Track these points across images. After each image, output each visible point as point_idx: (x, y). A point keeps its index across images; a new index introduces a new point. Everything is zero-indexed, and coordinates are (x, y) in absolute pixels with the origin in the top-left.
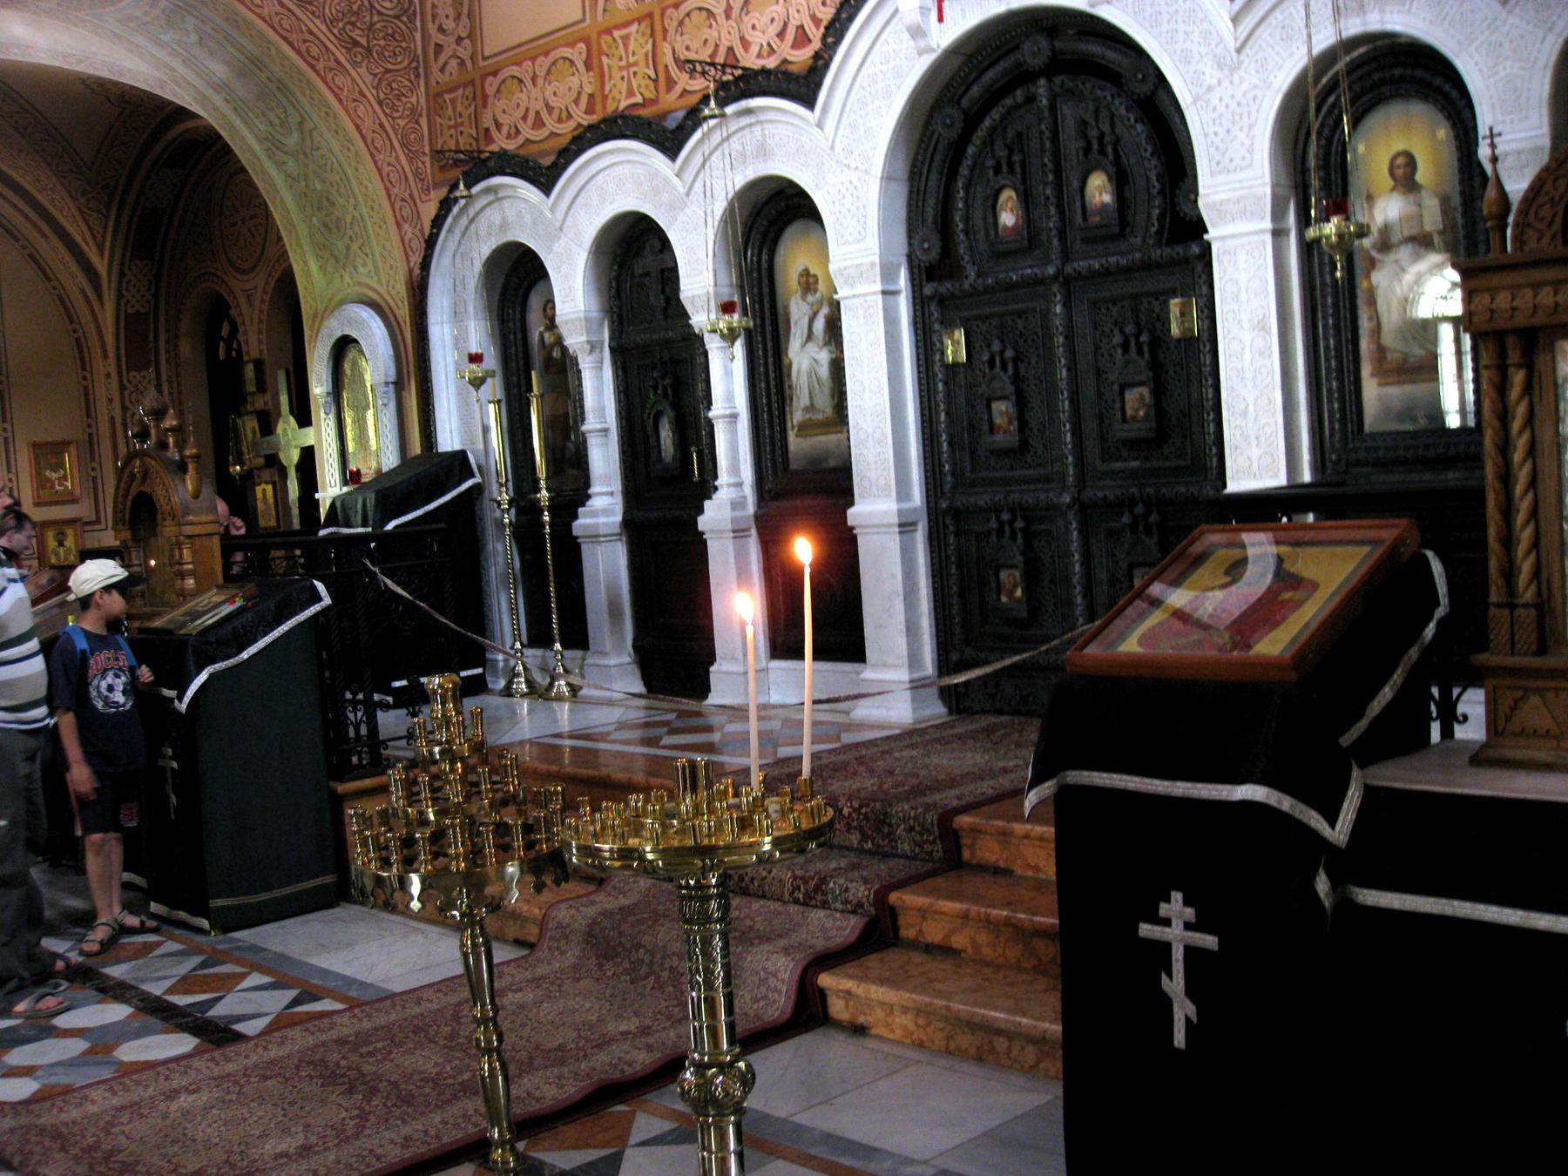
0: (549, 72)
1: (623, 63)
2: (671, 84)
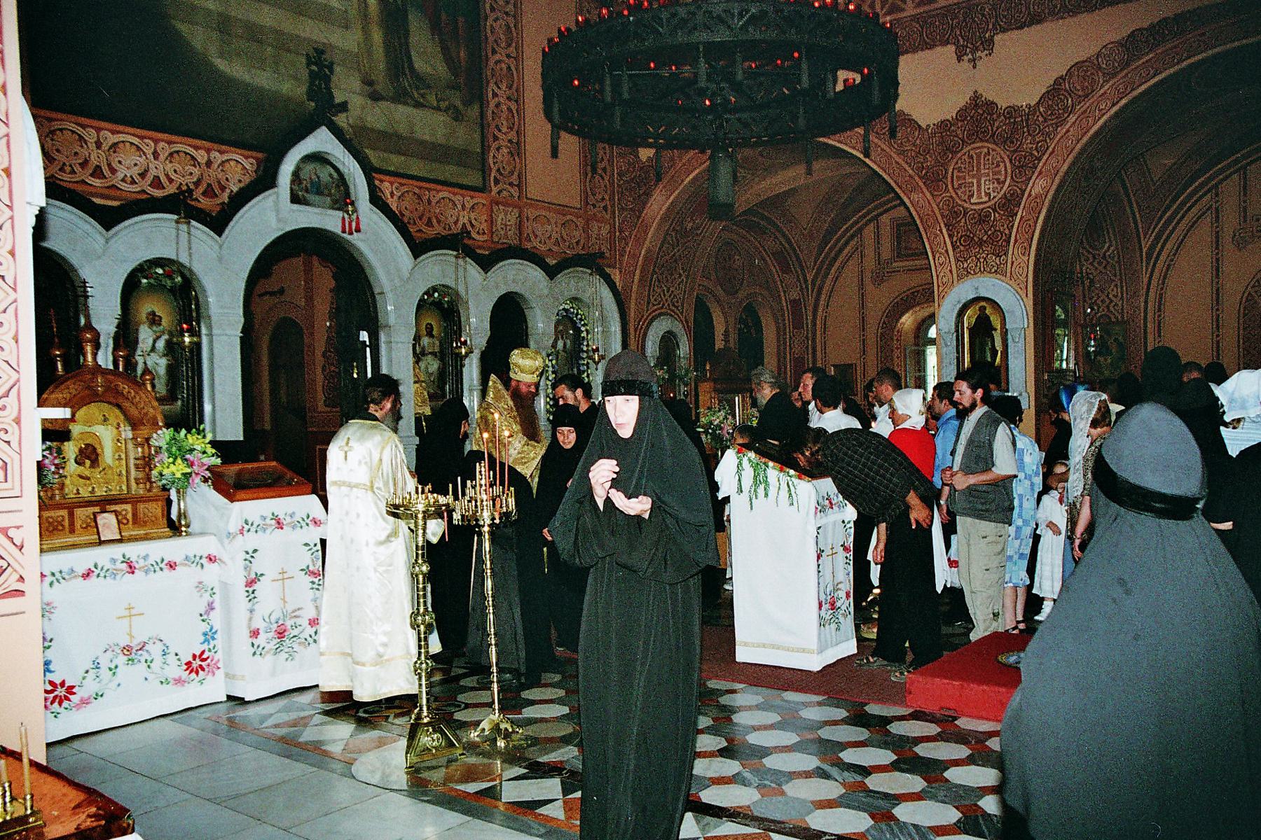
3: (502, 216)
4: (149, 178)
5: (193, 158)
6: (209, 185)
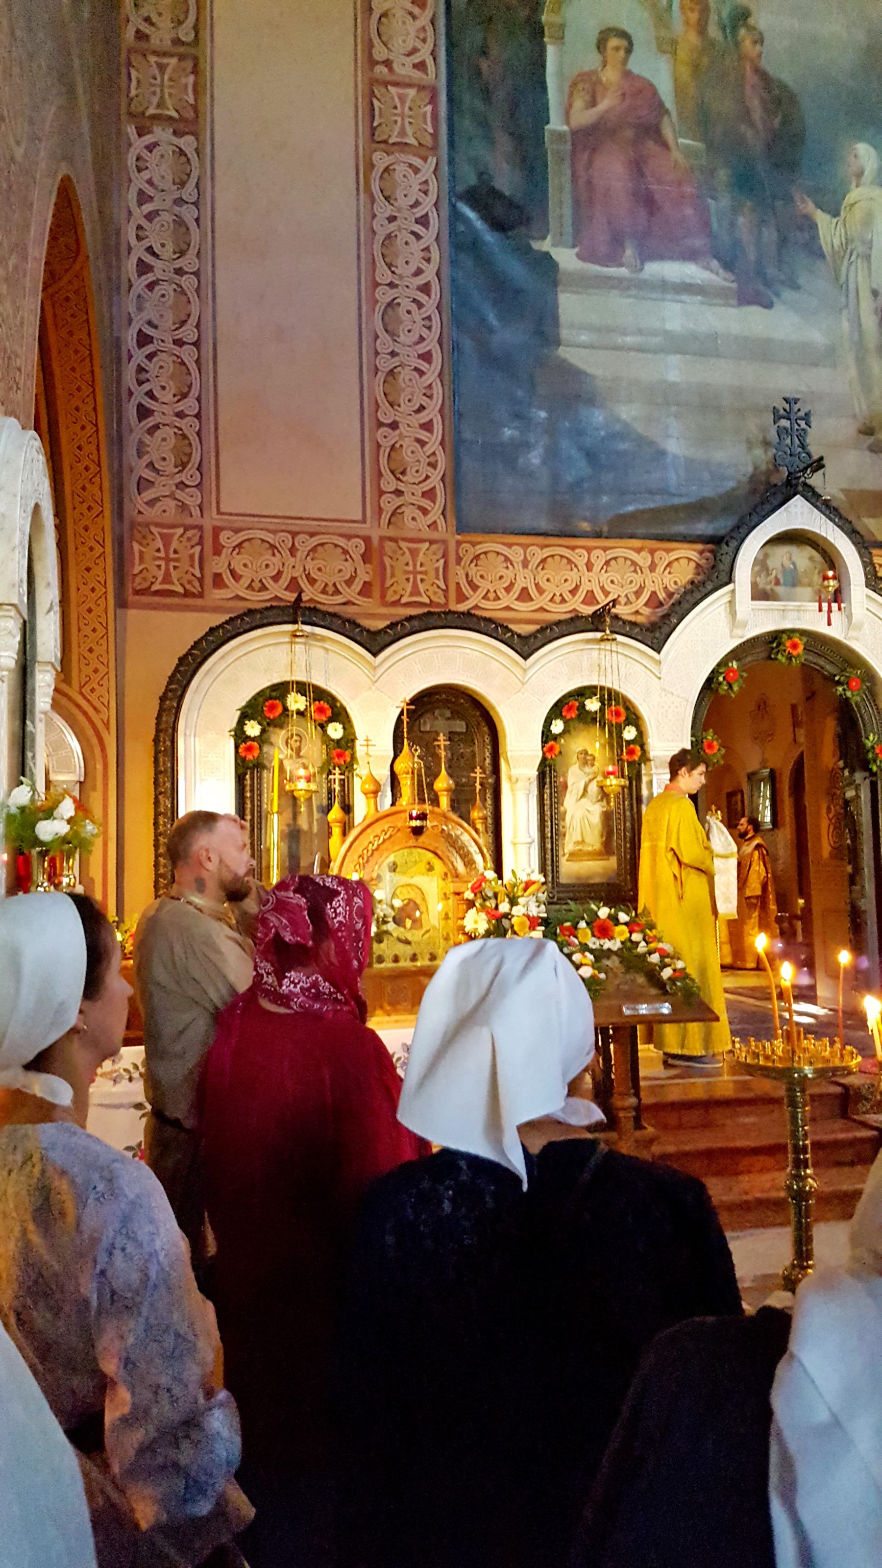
0: (314, 549)
1: (411, 568)
4: (581, 595)
5: (634, 563)
6: (654, 593)
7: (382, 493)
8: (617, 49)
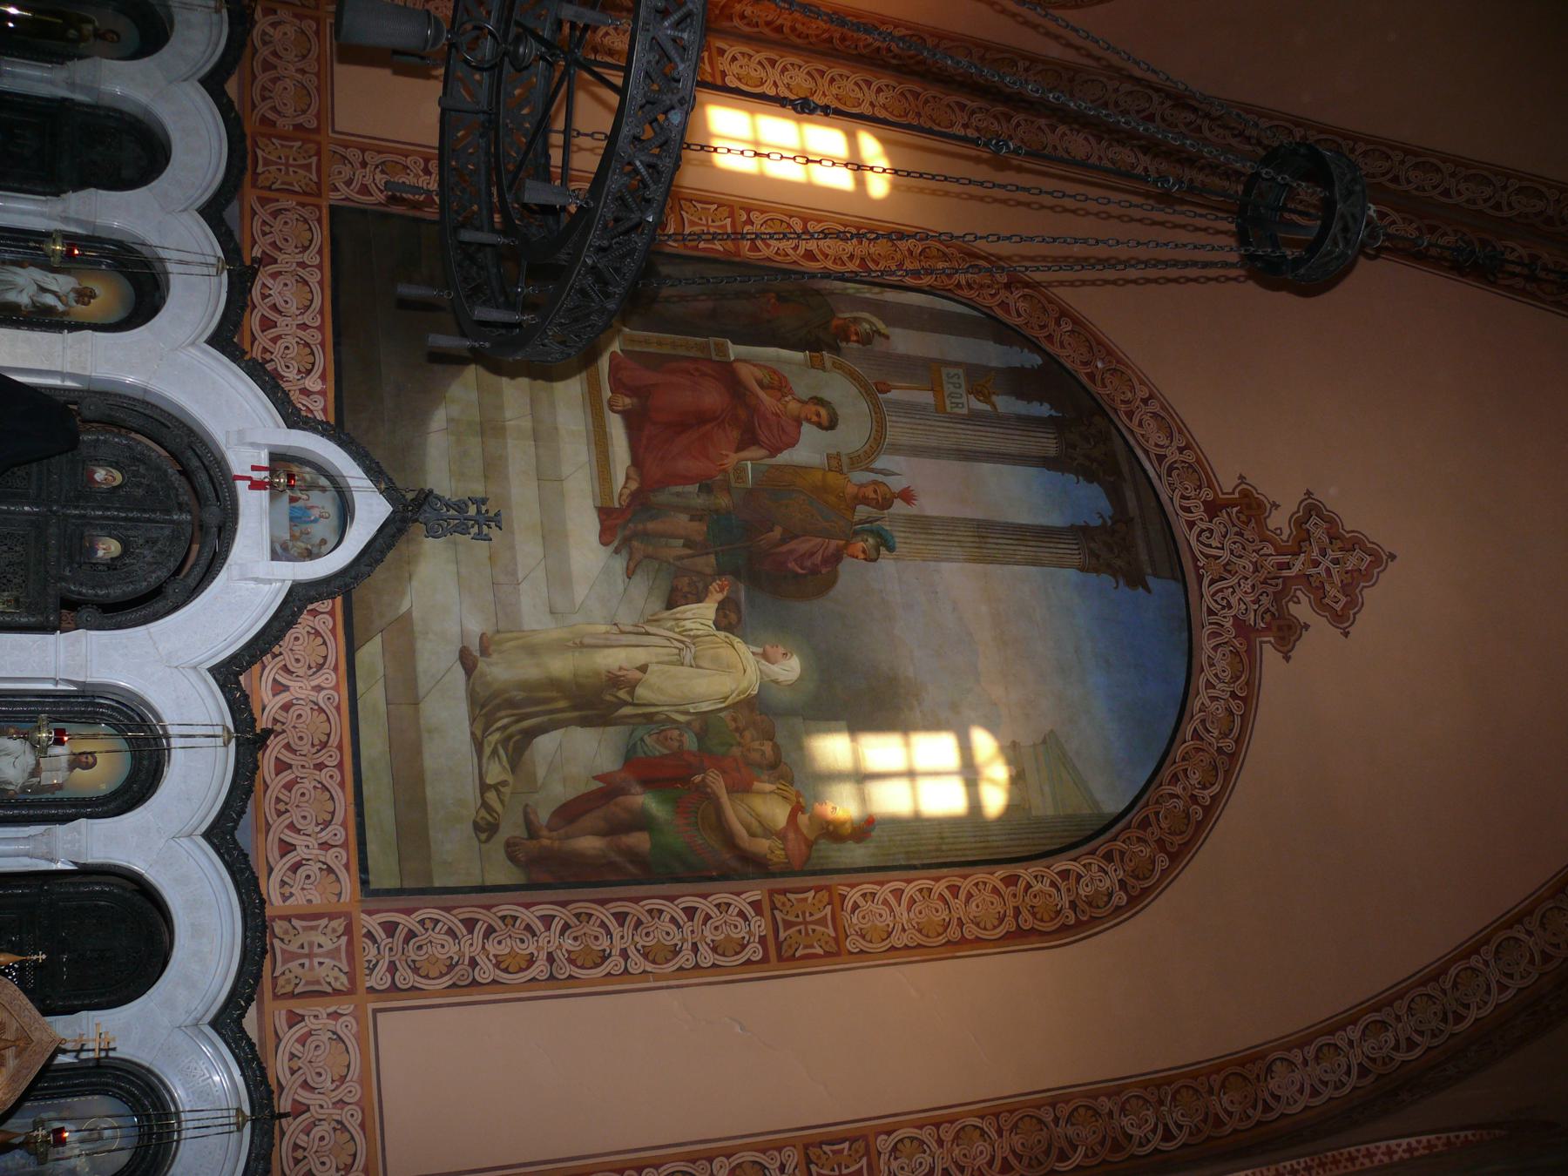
2: (263, 201)
3: (328, 945)
7: (363, 151)
8: (818, 415)
